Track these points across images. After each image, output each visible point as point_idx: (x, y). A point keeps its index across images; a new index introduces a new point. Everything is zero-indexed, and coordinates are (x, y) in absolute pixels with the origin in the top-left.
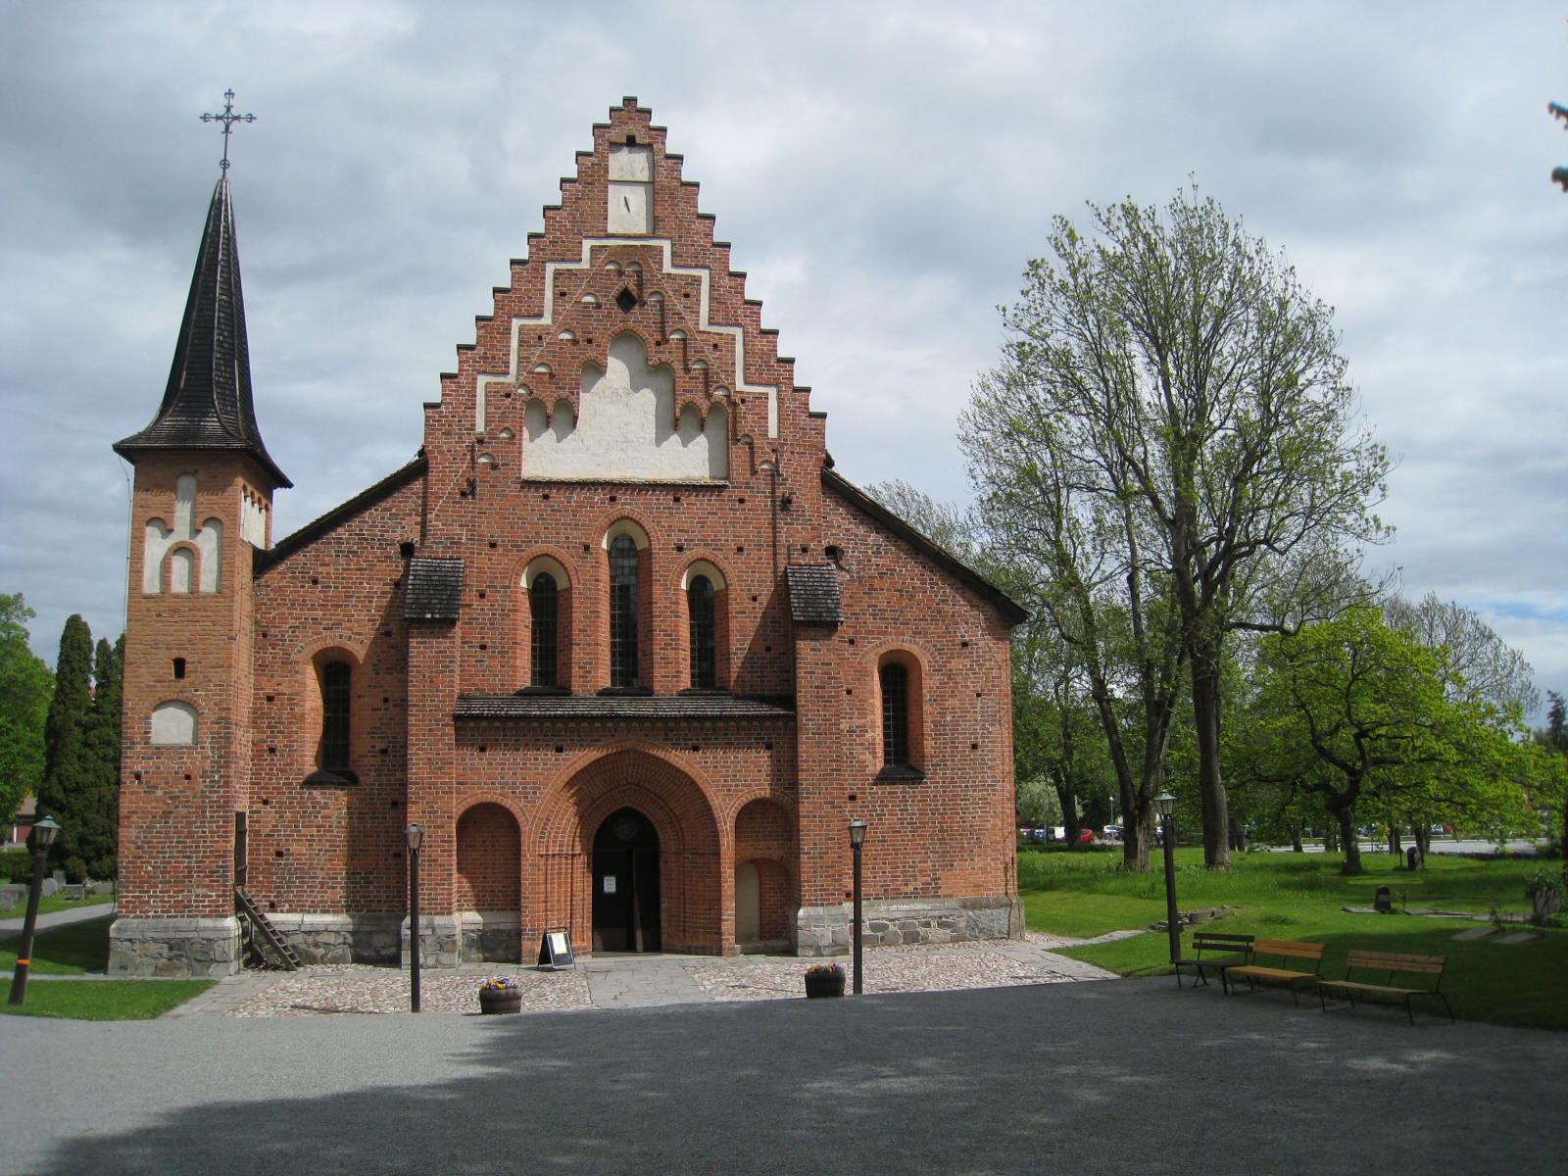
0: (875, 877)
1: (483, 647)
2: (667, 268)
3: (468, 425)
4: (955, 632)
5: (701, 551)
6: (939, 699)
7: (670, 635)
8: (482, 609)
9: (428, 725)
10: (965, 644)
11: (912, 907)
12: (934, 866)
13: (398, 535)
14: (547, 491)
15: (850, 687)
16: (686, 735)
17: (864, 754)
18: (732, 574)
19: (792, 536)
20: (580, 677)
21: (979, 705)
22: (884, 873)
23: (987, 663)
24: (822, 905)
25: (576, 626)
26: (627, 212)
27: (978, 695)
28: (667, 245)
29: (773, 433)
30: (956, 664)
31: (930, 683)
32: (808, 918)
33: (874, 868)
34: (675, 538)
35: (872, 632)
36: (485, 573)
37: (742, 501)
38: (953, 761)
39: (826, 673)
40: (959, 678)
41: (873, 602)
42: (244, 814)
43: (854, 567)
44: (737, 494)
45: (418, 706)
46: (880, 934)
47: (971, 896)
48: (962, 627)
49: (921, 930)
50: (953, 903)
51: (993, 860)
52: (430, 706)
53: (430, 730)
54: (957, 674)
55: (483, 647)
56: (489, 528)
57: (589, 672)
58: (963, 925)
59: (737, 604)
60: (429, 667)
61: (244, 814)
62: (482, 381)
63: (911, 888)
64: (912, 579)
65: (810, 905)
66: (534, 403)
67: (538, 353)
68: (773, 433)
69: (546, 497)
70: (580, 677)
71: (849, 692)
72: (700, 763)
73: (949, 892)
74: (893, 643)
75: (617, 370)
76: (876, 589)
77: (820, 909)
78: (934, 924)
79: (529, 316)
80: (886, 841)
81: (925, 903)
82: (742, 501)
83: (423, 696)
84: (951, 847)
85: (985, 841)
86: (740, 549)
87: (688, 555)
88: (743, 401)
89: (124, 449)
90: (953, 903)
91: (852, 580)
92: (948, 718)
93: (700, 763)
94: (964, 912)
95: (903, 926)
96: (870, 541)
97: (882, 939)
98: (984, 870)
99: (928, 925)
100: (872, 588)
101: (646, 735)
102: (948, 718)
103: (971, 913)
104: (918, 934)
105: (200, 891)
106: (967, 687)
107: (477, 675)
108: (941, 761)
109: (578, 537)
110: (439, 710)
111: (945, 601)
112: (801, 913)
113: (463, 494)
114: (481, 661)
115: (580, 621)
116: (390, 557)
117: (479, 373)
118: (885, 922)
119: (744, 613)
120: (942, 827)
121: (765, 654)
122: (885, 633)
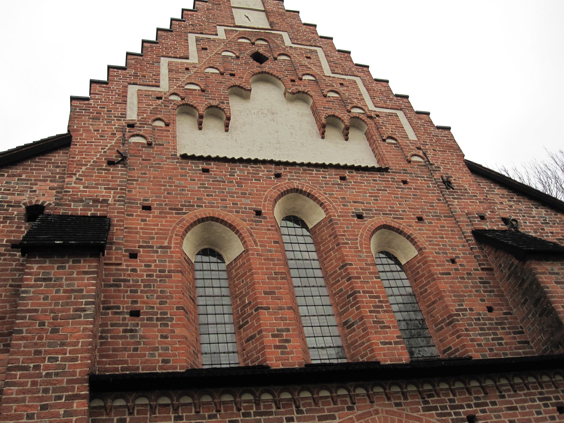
5: (382, 220)
7: (378, 297)
8: (134, 270)
9: (41, 399)
13: (25, 198)
14: (205, 166)
16: (451, 401)
18: (421, 240)
19: (464, 208)
20: (276, 347)
25: (260, 288)
29: (412, 136)
34: (352, 208)
36: (137, 233)
37: (405, 182)
45: (27, 368)
52: (46, 368)
53: (43, 407)
55: (135, 314)
57: (288, 341)
59: (438, 266)
60: (52, 311)
67: (187, 76)
69: (205, 171)
70: (276, 347)
82: (405, 182)
83: (38, 353)
87: (371, 222)
101: (397, 405)
107: (125, 349)
110: (64, 374)
113: (111, 163)
114: (131, 331)
115: (264, 283)
116: (11, 219)
117: (130, 84)
119: (450, 274)
121: (489, 315)
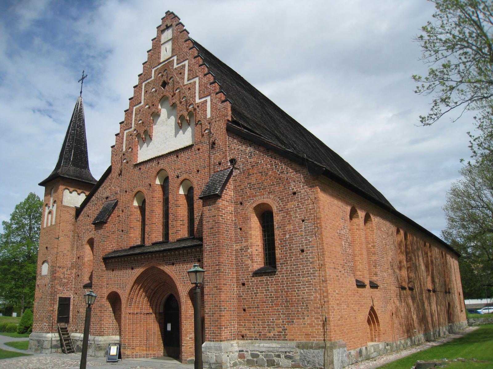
0: (254, 328)
1: (122, 231)
2: (175, 66)
3: (121, 150)
4: (289, 188)
6: (282, 226)
10: (294, 193)
11: (271, 345)
12: (283, 322)
15: (240, 226)
16: (170, 258)
17: (248, 260)
21: (303, 226)
22: (259, 325)
23: (306, 202)
24: (213, 341)
26: (166, 52)
27: (303, 221)
28: (175, 58)
30: (290, 205)
31: (277, 219)
32: (206, 347)
33: (254, 323)
35: (250, 197)
38: (291, 260)
39: (214, 221)
40: (292, 213)
41: (250, 181)
42: (68, 299)
43: (241, 166)
44: (197, 147)
46: (255, 359)
47: (304, 341)
48: (292, 184)
49: (276, 359)
50: (293, 344)
51: (315, 319)
54: (291, 211)
56: (125, 186)
58: (298, 358)
61: (68, 299)
62: (126, 132)
63: (272, 334)
64: (266, 165)
65: (209, 341)
66: (138, 135)
68: (209, 116)
71: (241, 229)
72: (174, 271)
73: (292, 337)
74: (260, 200)
75: (164, 112)
76: (251, 175)
77: (212, 343)
78: (283, 356)
79: (138, 104)
80: (259, 308)
81: (278, 343)
84: (292, 311)
85: (311, 308)
86: (198, 171)
88: (198, 107)
89: (41, 184)
90: (293, 344)
91: (240, 173)
92: (288, 236)
93: (174, 271)
94: (298, 350)
95: (266, 356)
96: (247, 151)
97: (257, 362)
98: (311, 325)
99: (279, 356)
100: (249, 175)
102: (288, 236)
103: (302, 351)
104: (274, 361)
105: (45, 324)
106: (296, 217)
108: (285, 261)
109: (148, 181)
111: (282, 173)
112: (203, 345)
118: (257, 353)
120: (287, 299)
122: (255, 196)
